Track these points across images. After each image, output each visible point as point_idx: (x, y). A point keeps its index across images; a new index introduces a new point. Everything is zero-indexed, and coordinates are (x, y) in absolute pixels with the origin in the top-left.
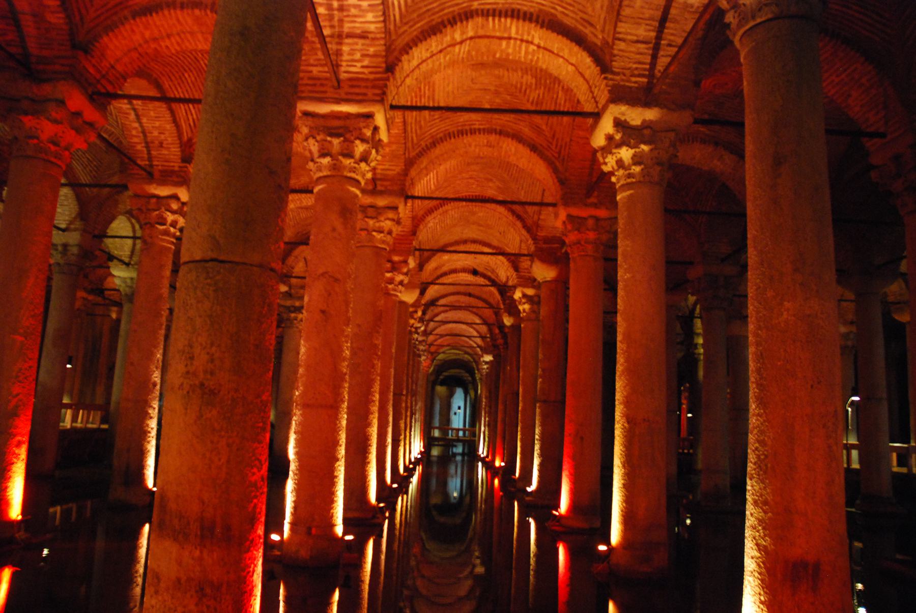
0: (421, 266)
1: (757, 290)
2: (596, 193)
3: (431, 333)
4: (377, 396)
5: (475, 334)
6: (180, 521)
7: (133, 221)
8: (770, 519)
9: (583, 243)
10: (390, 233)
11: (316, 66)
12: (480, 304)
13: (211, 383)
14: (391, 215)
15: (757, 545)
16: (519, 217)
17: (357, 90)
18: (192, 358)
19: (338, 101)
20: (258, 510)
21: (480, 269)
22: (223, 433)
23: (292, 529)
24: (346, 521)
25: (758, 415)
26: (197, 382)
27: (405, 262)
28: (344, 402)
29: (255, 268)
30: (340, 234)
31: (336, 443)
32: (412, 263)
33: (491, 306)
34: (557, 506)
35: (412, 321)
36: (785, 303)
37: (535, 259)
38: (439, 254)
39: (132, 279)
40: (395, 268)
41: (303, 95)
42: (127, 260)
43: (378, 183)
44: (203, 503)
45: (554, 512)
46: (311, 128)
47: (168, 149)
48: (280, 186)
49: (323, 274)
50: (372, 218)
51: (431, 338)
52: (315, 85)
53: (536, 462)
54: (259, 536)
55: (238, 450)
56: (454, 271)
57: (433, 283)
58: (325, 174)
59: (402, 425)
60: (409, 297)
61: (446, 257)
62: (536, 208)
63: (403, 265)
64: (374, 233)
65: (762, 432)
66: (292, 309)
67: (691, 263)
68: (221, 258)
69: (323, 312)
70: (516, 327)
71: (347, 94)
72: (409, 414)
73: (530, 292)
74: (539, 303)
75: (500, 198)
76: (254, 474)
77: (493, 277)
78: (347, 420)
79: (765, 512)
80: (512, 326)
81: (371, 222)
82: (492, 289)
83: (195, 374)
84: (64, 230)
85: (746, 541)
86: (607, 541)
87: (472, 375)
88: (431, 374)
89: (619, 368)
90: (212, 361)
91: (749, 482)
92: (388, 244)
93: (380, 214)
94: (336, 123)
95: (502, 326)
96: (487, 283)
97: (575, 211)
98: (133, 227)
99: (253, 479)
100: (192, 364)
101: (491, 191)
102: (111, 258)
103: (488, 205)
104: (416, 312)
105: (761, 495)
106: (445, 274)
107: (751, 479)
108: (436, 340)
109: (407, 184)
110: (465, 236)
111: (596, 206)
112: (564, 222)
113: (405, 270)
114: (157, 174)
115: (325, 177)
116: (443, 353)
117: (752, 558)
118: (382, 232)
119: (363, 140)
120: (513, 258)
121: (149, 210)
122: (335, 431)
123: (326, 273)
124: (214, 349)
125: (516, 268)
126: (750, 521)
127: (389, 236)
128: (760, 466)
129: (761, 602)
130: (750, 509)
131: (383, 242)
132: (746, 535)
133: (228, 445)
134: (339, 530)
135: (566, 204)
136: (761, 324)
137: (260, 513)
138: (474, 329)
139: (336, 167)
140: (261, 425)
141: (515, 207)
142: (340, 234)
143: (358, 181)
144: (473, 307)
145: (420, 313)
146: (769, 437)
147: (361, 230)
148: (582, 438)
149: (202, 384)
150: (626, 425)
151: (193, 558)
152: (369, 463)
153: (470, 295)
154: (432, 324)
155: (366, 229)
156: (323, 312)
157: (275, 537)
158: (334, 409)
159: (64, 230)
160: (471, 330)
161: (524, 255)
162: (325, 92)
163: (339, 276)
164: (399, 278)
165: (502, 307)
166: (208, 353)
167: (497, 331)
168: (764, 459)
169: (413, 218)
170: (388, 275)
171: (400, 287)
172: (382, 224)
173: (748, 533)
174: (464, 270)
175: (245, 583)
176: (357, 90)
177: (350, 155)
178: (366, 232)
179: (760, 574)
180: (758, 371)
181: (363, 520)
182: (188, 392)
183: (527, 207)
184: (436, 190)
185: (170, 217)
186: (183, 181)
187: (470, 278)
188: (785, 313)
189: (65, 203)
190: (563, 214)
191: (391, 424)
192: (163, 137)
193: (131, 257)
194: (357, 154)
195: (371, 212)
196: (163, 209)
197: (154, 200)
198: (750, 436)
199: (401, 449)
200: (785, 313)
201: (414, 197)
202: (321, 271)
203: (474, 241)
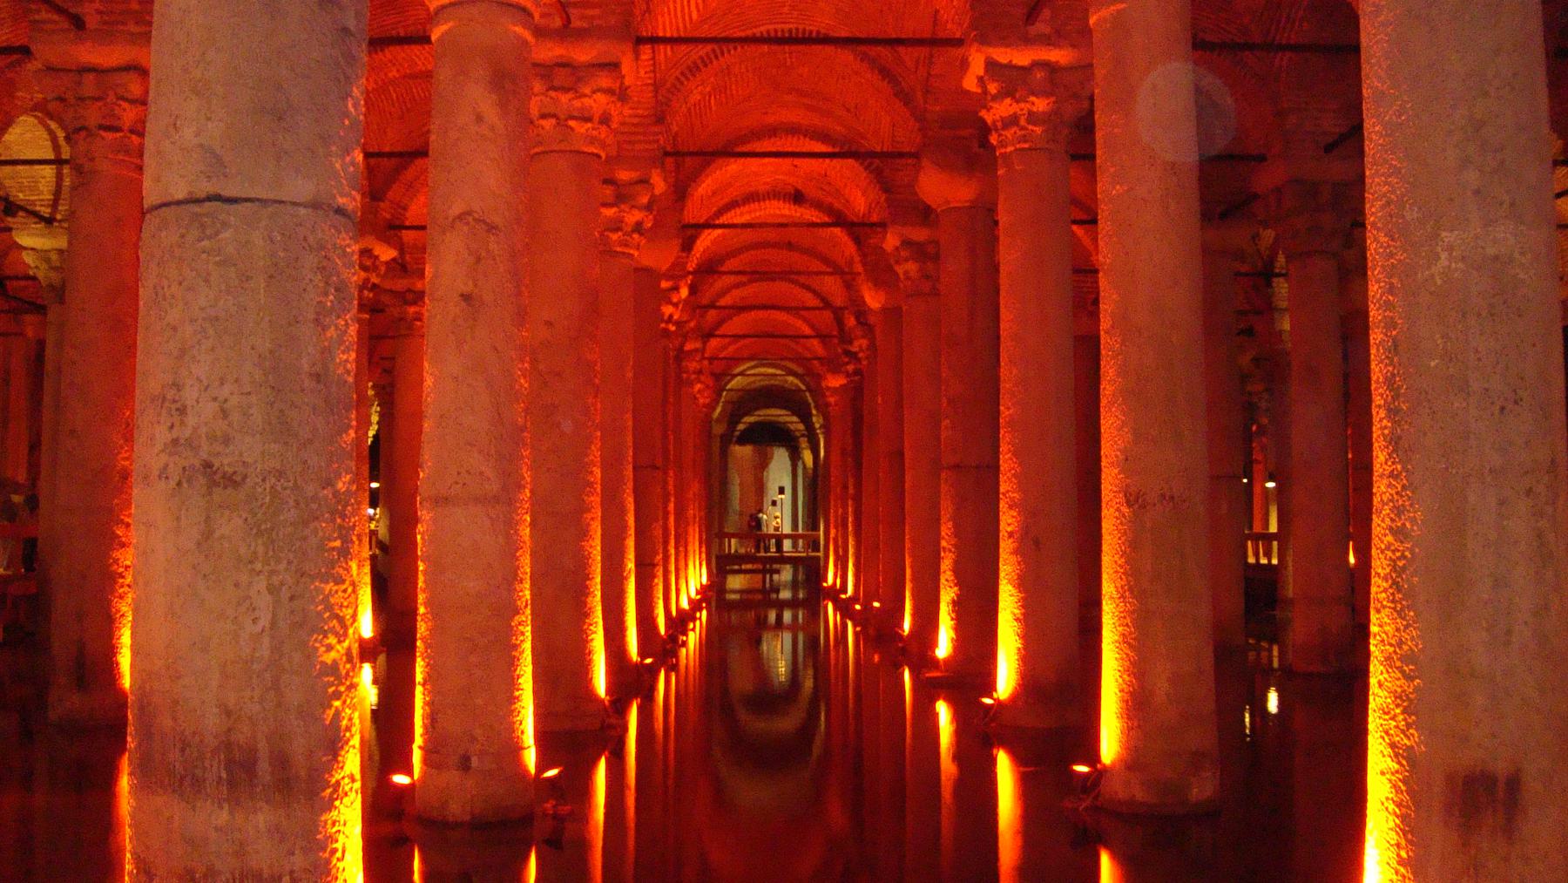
0: (680, 192)
1: (1383, 207)
2: (1046, 13)
3: (710, 335)
4: (597, 471)
5: (807, 331)
6: (183, 750)
7: (53, 125)
8: (1416, 689)
9: (1023, 122)
10: (605, 120)
12: (816, 265)
13: (226, 461)
14: (604, 81)
15: (1393, 745)
16: (885, 73)
18: (182, 411)
20: (344, 723)
21: (811, 192)
22: (258, 566)
23: (426, 761)
24: (542, 738)
25: (1391, 475)
26: (197, 463)
27: (644, 181)
28: (520, 487)
29: (302, 211)
30: (492, 128)
31: (513, 578)
32: (659, 184)
33: (837, 271)
34: (989, 686)
35: (668, 310)
36: (1444, 234)
37: (925, 162)
38: (720, 161)
39: (60, 252)
40: (622, 197)
42: (46, 211)
43: (573, 12)
44: (228, 713)
45: (987, 701)
48: (345, 30)
49: (460, 217)
50: (566, 90)
51: (714, 342)
53: (947, 596)
54: (353, 780)
55: (292, 598)
56: (752, 198)
57: (708, 225)
59: (658, 532)
60: (658, 256)
61: (734, 167)
62: (923, 52)
63: (639, 187)
64: (572, 123)
65: (1398, 511)
66: (410, 297)
67: (1262, 159)
68: (227, 193)
69: (467, 297)
70: (892, 314)
72: (671, 506)
73: (920, 235)
74: (936, 258)
75: (844, 34)
76: (330, 648)
77: (837, 205)
78: (533, 524)
79: (1408, 678)
80: (883, 309)
81: (564, 98)
82: (837, 231)
83: (191, 444)
85: (1370, 738)
86: (1092, 756)
87: (805, 418)
88: (718, 420)
89: (1107, 389)
90: (225, 413)
91: (1374, 617)
92: (603, 145)
93: (579, 79)
95: (861, 313)
96: (827, 219)
97: (1002, 55)
98: (54, 140)
99: (329, 658)
100: (182, 423)
101: (823, 21)
102: (11, 208)
103: (817, 48)
104: (676, 289)
105: (1400, 644)
106: (733, 205)
107: (1378, 611)
108: (725, 348)
109: (637, 12)
110: (770, 120)
111: (1047, 41)
112: (980, 79)
113: (645, 200)
114: (92, 22)
116: (742, 374)
117: (1383, 773)
118: (589, 120)
120: (877, 162)
121: (82, 99)
122: (510, 553)
123: (469, 213)
124: (225, 391)
125: (886, 185)
126: (1378, 698)
127: (604, 128)
128: (1395, 583)
129: (1401, 862)
130: (1377, 673)
131: (592, 141)
132: (1371, 727)
133: (271, 590)
134: (530, 758)
135: (984, 40)
136: (1394, 281)
137: (348, 729)
138: (805, 320)
140: (337, 544)
141: (874, 51)
142: (492, 128)
143: (524, 9)
144: (799, 273)
145: (684, 292)
146: (1413, 520)
147: (543, 116)
148: (1037, 543)
150: (1125, 510)
151: (216, 829)
152: (587, 615)
153: (790, 246)
154: (712, 315)
155: (554, 116)
156: (467, 297)
157: (400, 779)
158: (505, 498)
160: (799, 323)
161: (901, 155)
163: (497, 220)
164: (633, 217)
165: (859, 268)
166: (215, 399)
167: (851, 321)
168: (1404, 569)
169: (657, 87)
170: (610, 212)
171: (636, 236)
172: (586, 101)
173: (1374, 722)
174: (774, 194)
175: (329, 873)
178: (553, 121)
179: (1399, 805)
180: (1390, 382)
181: (576, 732)
182: (179, 484)
183: (901, 49)
184: (703, 22)
187: (786, 210)
188: (1444, 256)
190: (977, 65)
191: (632, 532)
193: (55, 204)
195: (561, 77)
198: (1376, 520)
199: (659, 581)
200: (1444, 256)
201: (654, 40)
202: (456, 209)
203: (794, 130)
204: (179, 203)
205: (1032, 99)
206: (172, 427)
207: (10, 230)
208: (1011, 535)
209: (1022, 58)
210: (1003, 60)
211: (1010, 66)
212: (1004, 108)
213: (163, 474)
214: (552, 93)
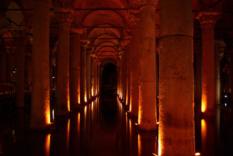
9: (208, 24)
18: (176, 68)
26: (179, 76)
49: (147, 38)
58: (145, 3)
69: (148, 50)
84: (19, 26)
97: (206, 13)
112: (201, 17)
115: (145, 4)
147: (135, 22)
149: (181, 77)
157: (136, 124)
159: (19, 26)
182: (176, 79)
185: (69, 20)
189: (19, 16)
202: (146, 37)
204: (173, 36)
205: (210, 20)
206: (174, 71)
207: (29, 38)
208: (205, 87)
209: (208, 14)
210: (205, 14)
211: (206, 15)
212: (205, 22)
213: (173, 78)
214: (137, 18)
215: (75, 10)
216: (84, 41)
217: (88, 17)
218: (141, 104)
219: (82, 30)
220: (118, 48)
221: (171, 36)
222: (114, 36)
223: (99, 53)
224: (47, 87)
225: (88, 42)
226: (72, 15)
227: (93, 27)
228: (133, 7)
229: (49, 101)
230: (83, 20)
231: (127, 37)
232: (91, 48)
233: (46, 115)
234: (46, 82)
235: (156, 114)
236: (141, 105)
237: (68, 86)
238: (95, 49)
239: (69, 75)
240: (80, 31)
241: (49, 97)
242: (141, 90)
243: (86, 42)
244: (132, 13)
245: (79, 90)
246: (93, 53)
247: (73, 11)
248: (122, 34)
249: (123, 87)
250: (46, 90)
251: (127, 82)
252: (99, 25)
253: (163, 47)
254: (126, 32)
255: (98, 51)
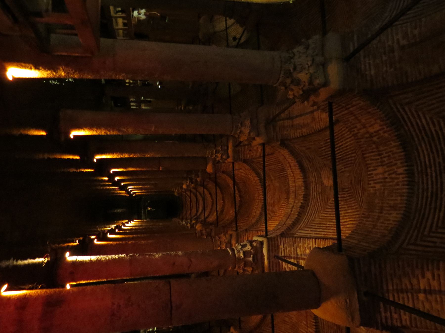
11: (284, 247)
17: (274, 266)
19: (269, 258)
41: (270, 242)
46: (256, 247)
47: (249, 153)
49: (191, 261)
52: (275, 247)
58: (236, 255)
69: (174, 264)
71: (273, 262)
94: (259, 256)
115: (235, 254)
119: (252, 271)
139: (239, 258)
147: (220, 242)
155: (221, 244)
156: (174, 264)
162: (272, 251)
176: (274, 266)
177: (245, 265)
185: (219, 155)
186: (235, 160)
192: (254, 151)
194: (246, 268)
196: (222, 152)
197: (226, 148)
202: (192, 260)
214: (225, 244)
215: (233, 163)
216: (199, 174)
217: (229, 178)
218: (99, 259)
219: (211, 171)
220: (195, 219)
221: (171, 297)
222: (210, 212)
223: (188, 193)
224: (122, 131)
225: (199, 179)
226: (226, 159)
227: (217, 184)
228: (240, 239)
229: (103, 133)
230: (224, 172)
231: (204, 232)
232: (192, 183)
233: (84, 130)
234: (129, 130)
235: (83, 282)
236: (97, 260)
237: (132, 156)
238: (193, 188)
239: (147, 156)
240: (210, 169)
241: (108, 133)
242: (119, 257)
243: (198, 177)
244: (231, 238)
245: (130, 169)
246: (188, 186)
247: (230, 160)
248: (211, 224)
249: (139, 229)
250: (119, 131)
251: (143, 235)
252: (222, 193)
253: (157, 286)
254: (211, 230)
255: (191, 191)
